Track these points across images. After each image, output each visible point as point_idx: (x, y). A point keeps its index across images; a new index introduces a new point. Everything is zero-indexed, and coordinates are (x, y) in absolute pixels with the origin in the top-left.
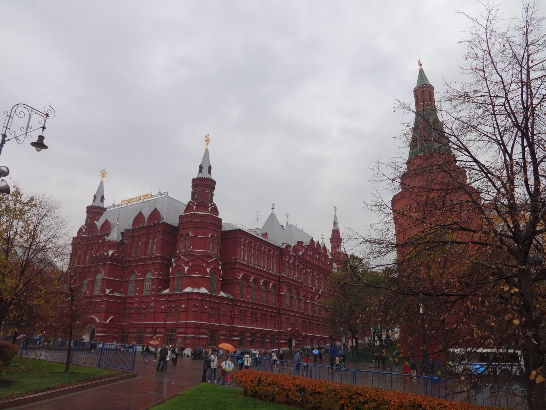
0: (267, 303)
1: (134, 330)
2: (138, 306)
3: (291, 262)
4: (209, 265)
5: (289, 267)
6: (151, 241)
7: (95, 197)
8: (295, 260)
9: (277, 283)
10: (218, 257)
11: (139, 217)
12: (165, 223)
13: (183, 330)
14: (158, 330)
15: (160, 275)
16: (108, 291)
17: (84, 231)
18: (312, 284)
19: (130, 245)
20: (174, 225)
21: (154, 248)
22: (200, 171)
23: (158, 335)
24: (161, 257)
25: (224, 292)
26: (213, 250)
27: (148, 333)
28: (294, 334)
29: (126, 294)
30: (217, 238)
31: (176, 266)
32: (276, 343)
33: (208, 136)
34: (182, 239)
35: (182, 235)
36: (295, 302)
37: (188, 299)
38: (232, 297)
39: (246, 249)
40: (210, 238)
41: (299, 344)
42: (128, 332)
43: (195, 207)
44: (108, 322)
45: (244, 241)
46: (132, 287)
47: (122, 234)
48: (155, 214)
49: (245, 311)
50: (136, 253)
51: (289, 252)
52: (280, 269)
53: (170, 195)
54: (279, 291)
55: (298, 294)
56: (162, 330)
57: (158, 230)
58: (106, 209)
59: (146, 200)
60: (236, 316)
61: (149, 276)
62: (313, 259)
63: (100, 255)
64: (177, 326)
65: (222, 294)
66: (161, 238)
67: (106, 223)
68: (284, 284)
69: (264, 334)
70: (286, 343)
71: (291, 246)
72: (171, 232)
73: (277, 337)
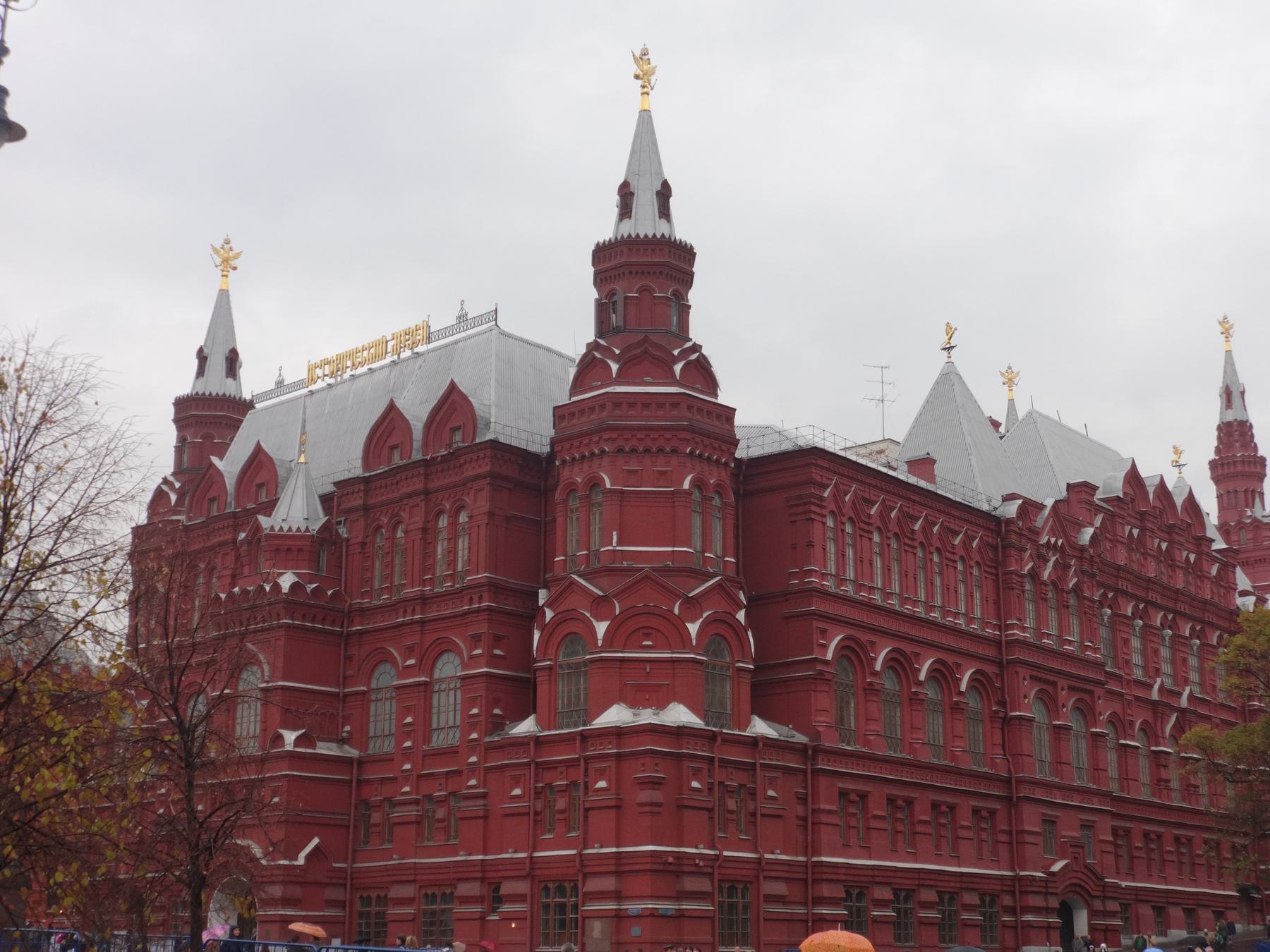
0: (953, 757)
1: (409, 891)
3: (1046, 574)
4: (693, 606)
5: (1041, 599)
6: (443, 522)
7: (202, 357)
8: (1061, 567)
9: (990, 670)
10: (731, 573)
11: (390, 424)
12: (494, 444)
13: (609, 883)
15: (492, 660)
16: (290, 737)
17: (173, 497)
18: (1145, 668)
19: (363, 544)
20: (534, 448)
21: (461, 551)
22: (625, 210)
23: (506, 908)
25: (764, 717)
26: (708, 542)
28: (1084, 887)
29: (363, 746)
30: (720, 490)
31: (559, 621)
32: (1005, 926)
33: (645, 53)
34: (574, 503)
35: (572, 488)
36: (1078, 751)
37: (619, 756)
38: (801, 738)
39: (849, 529)
40: (688, 493)
41: (1107, 929)
42: (383, 900)
43: (614, 367)
44: (301, 860)
45: (838, 496)
46: (383, 718)
47: (326, 500)
48: (453, 407)
49: (863, 796)
50: (389, 577)
51: (1037, 532)
52: (1001, 607)
53: (504, 324)
55: (1086, 711)
56: (522, 887)
57: (469, 473)
58: (249, 405)
59: (406, 354)
60: (823, 818)
61: (448, 667)
62: (1145, 555)
63: (245, 592)
64: (585, 867)
65: (760, 727)
66: (483, 504)
67: (259, 460)
68: (1022, 671)
69: (950, 890)
70: (1049, 927)
71: (1041, 507)
72: (526, 480)
73: (1007, 900)
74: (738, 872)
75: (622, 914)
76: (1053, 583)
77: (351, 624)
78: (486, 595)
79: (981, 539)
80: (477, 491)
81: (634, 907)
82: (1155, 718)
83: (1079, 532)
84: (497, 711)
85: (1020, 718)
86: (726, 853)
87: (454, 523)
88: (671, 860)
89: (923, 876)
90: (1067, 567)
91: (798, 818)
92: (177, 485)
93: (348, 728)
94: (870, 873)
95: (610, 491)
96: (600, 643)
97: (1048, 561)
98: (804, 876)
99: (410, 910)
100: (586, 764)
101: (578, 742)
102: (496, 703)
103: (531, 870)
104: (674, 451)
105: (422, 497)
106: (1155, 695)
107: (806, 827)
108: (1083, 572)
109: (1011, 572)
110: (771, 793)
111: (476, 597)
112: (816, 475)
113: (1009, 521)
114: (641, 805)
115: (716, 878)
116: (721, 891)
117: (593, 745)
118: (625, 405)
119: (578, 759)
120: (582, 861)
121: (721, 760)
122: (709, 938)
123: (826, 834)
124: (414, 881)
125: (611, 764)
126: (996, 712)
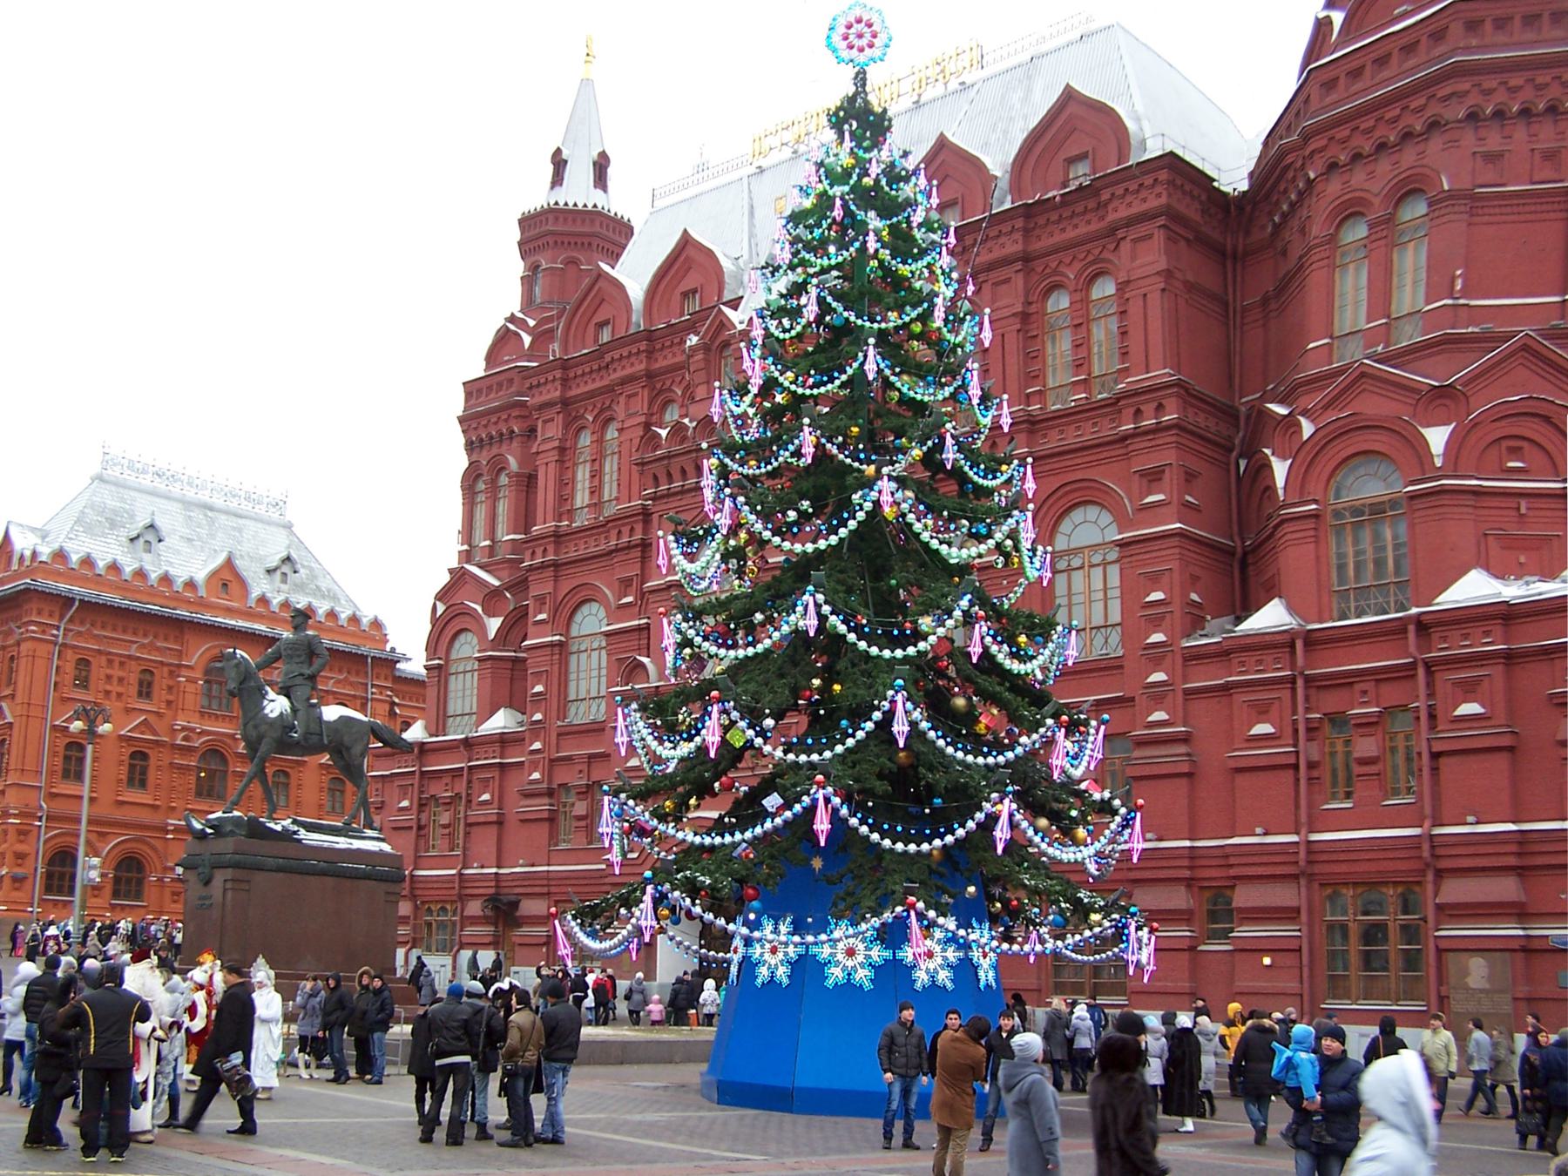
7: (559, 163)
13: (1505, 889)
14: (1244, 897)
17: (527, 340)
21: (1111, 334)
23: (1245, 931)
37: (1509, 658)
64: (1438, 861)
75: (1536, 945)
78: (1171, 403)
84: (1194, 597)
87: (1082, 303)
92: (532, 323)
96: (1438, 462)
101: (1411, 635)
103: (1310, 868)
105: (1018, 265)
111: (1148, 409)
117: (1445, 639)
125: (1496, 671)
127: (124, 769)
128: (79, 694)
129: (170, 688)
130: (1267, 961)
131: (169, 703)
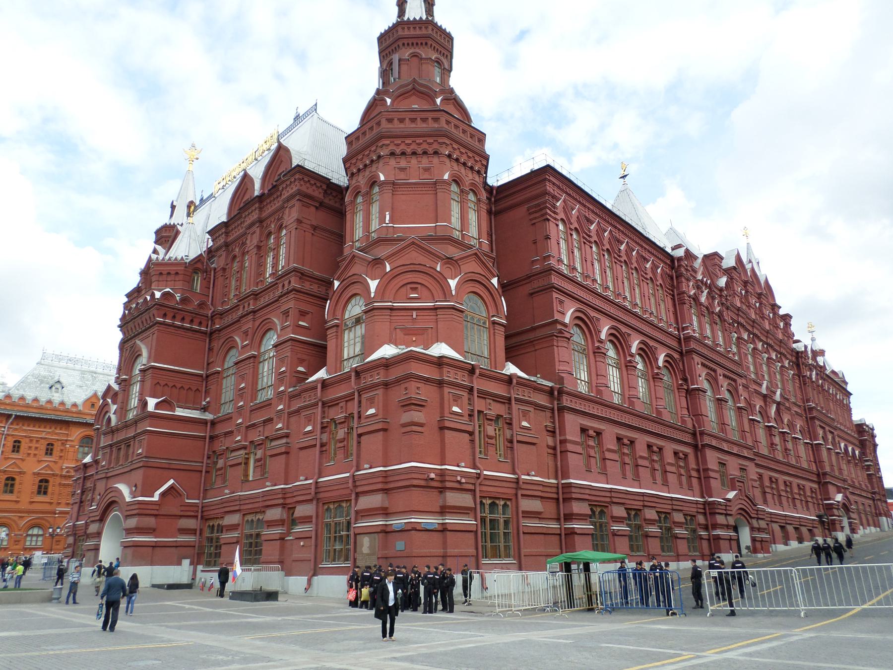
0: (659, 413)
2: (245, 438)
5: (700, 315)
7: (173, 207)
8: (711, 296)
9: (676, 356)
12: (300, 169)
16: (152, 403)
18: (756, 374)
19: (224, 269)
23: (298, 529)
24: (295, 270)
27: (271, 524)
31: (344, 289)
44: (156, 498)
45: (567, 209)
46: (229, 387)
52: (679, 317)
54: (685, 380)
57: (286, 195)
64: (357, 488)
68: (697, 359)
71: (696, 258)
73: (701, 519)
74: (499, 490)
75: (388, 530)
76: (707, 308)
77: (213, 324)
79: (662, 269)
80: (291, 208)
81: (398, 522)
82: (766, 405)
83: (717, 280)
84: (301, 369)
85: (698, 389)
86: (485, 473)
88: (433, 476)
89: (646, 499)
90: (713, 298)
91: (548, 447)
93: (208, 399)
94: (608, 494)
95: (384, 183)
97: (702, 292)
98: (555, 496)
99: (235, 534)
100: (360, 396)
101: (353, 378)
102: (301, 362)
103: (317, 495)
104: (436, 153)
106: (764, 391)
107: (555, 455)
108: (722, 304)
109: (684, 292)
110: (525, 424)
112: (549, 188)
113: (680, 259)
114: (404, 425)
115: (478, 494)
116: (482, 503)
118: (396, 121)
119: (353, 394)
120: (354, 482)
121: (479, 391)
122: (472, 551)
123: (572, 459)
124: (239, 510)
125: (380, 392)
126: (681, 385)
127: (36, 487)
128: (15, 455)
129: (62, 450)
130: (302, 544)
131: (61, 457)
